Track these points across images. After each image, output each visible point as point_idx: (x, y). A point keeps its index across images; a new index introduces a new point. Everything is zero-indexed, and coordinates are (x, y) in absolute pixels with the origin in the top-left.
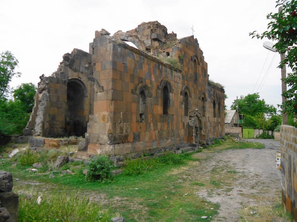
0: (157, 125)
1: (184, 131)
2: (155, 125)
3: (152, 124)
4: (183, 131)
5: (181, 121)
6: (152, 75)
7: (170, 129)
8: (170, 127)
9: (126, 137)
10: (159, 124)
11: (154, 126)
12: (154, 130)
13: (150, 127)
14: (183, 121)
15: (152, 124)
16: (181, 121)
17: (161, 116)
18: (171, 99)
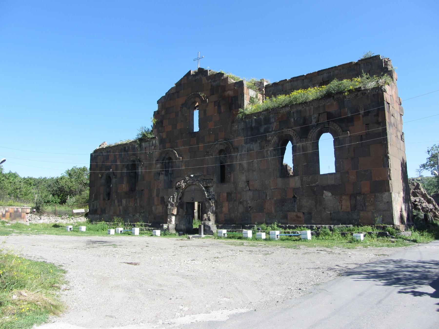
0: (121, 202)
1: (163, 208)
2: (120, 202)
3: (116, 201)
4: (161, 208)
5: (157, 195)
6: (118, 160)
7: (138, 205)
8: (138, 203)
9: (96, 210)
10: (124, 201)
11: (118, 202)
12: (119, 206)
13: (114, 203)
14: (161, 195)
15: (116, 201)
16: (157, 195)
17: (126, 193)
18: (140, 173)
